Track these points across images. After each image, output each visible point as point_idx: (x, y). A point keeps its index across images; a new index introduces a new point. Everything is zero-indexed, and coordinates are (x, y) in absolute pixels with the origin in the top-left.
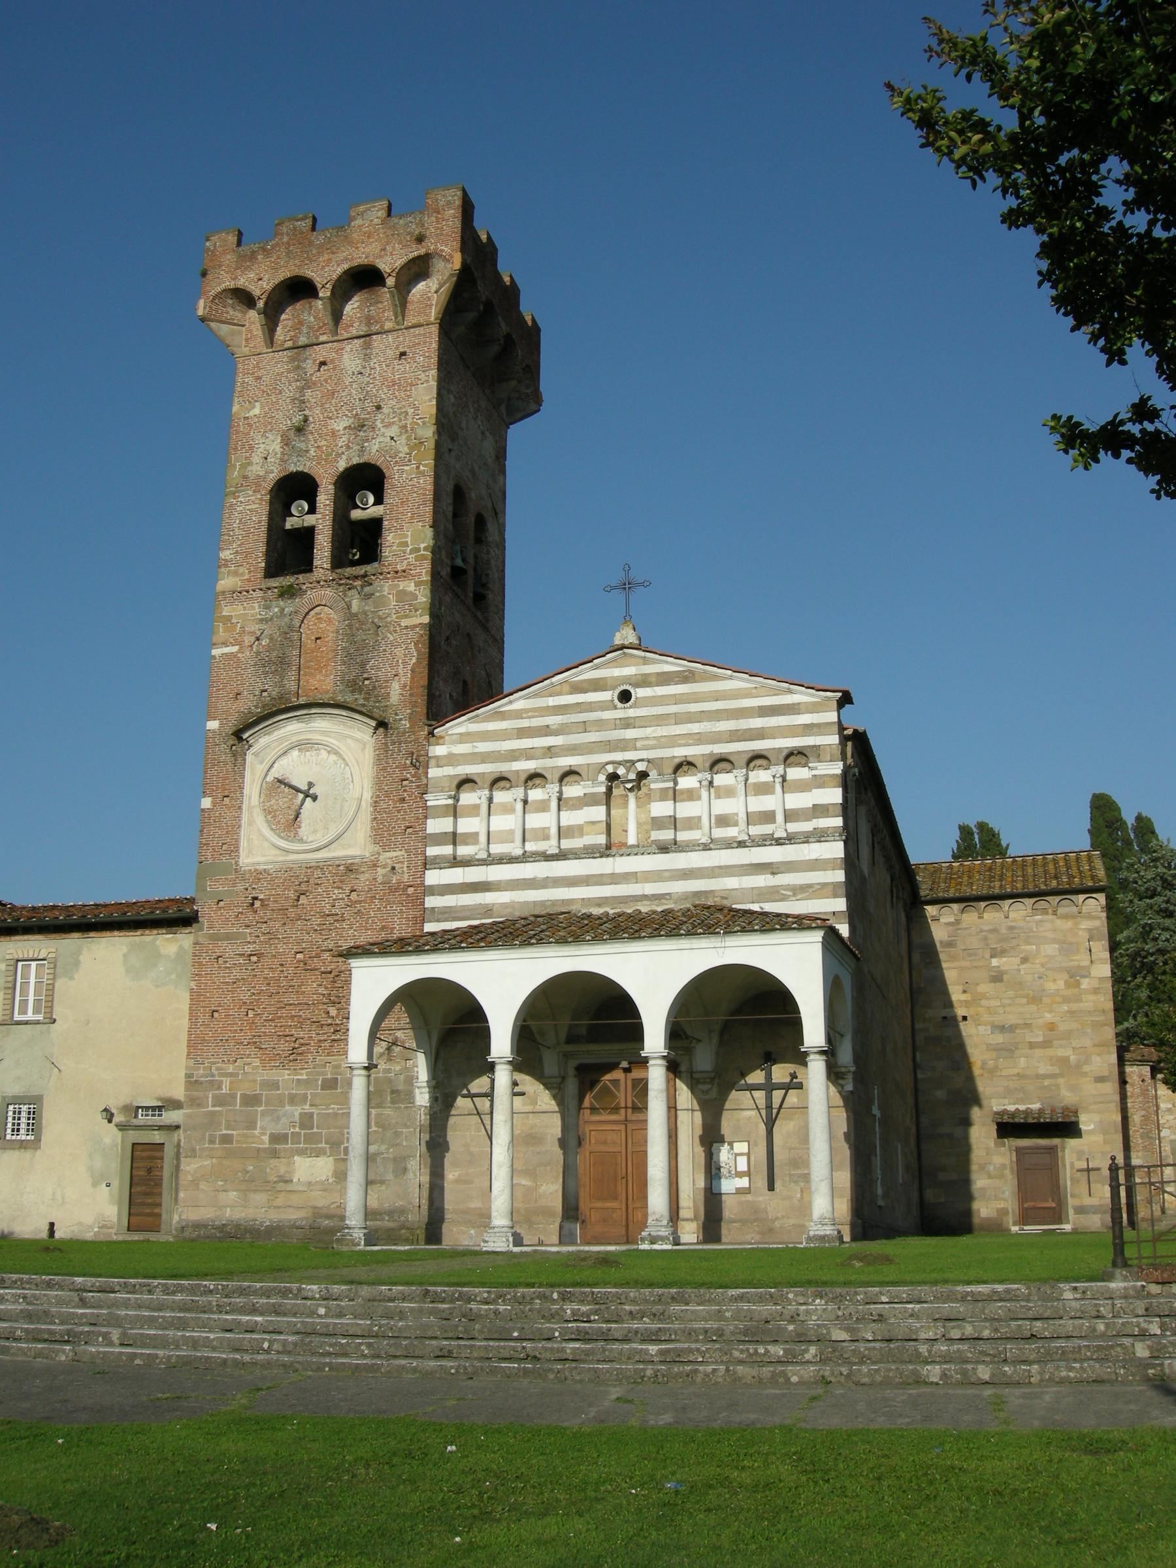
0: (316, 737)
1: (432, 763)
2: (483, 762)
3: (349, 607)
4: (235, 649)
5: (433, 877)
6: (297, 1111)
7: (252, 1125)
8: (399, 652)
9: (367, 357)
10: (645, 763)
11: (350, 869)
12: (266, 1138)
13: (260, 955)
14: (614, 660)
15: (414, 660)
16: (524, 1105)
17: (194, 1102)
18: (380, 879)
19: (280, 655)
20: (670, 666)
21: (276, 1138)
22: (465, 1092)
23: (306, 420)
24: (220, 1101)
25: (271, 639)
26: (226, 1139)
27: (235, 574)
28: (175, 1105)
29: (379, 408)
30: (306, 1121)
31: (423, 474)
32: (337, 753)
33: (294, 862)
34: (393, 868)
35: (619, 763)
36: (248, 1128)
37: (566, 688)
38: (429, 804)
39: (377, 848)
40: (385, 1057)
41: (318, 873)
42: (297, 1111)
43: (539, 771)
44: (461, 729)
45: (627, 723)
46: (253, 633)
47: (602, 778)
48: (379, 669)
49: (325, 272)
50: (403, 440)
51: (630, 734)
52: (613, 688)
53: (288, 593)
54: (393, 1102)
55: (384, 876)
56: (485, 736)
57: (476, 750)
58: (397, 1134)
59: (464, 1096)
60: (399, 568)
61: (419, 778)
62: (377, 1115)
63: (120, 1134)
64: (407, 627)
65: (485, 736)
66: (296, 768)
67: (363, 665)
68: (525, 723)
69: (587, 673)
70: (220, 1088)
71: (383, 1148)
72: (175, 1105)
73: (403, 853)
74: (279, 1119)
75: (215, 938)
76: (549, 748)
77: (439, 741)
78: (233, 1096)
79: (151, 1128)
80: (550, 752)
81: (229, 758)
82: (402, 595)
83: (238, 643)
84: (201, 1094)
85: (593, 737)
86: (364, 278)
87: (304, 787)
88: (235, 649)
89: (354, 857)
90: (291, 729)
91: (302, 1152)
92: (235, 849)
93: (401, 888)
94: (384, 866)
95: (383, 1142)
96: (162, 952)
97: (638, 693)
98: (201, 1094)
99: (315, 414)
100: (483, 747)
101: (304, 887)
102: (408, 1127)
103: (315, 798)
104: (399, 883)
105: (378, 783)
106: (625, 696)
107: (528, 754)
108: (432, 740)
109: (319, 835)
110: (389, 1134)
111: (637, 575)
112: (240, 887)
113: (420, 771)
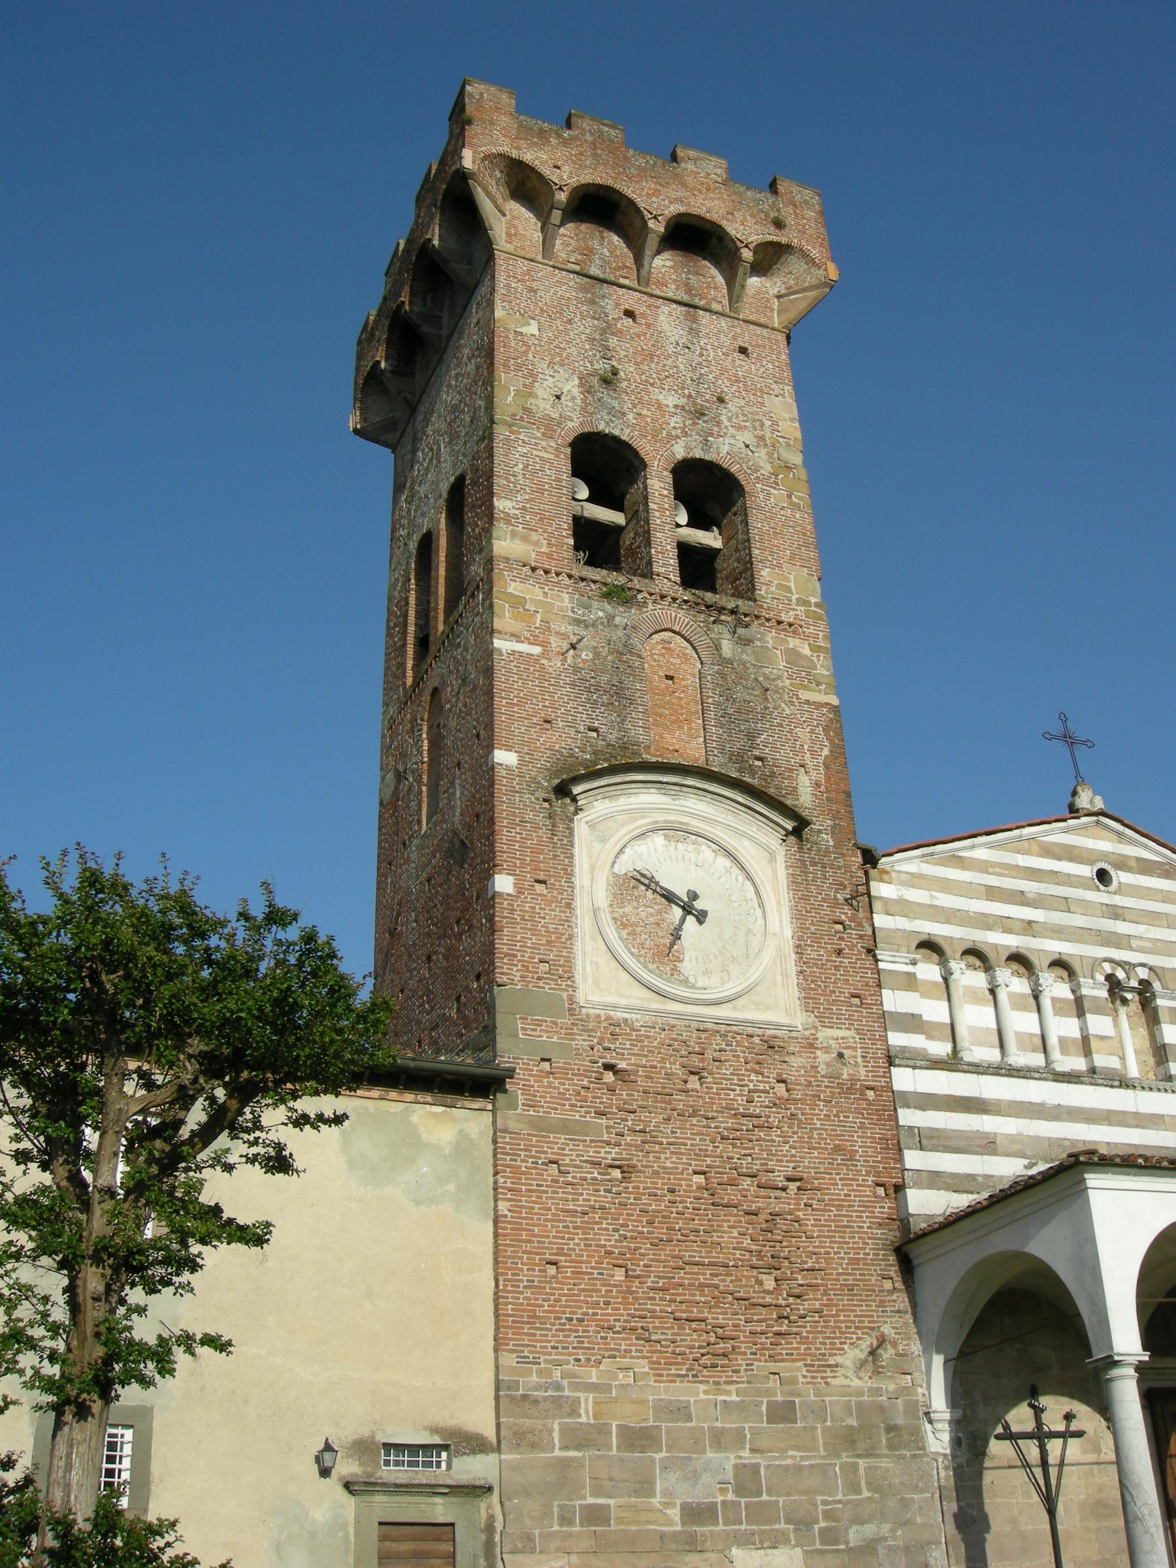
0: (695, 824)
1: (877, 906)
2: (947, 921)
3: (718, 647)
4: (536, 650)
5: (904, 1079)
6: (728, 1461)
7: (645, 1487)
8: (803, 734)
9: (694, 332)
10: (1147, 970)
11: (770, 1046)
12: (675, 1513)
13: (627, 1170)
14: (1085, 827)
15: (826, 752)
16: (1084, 1452)
17: (526, 1440)
18: (823, 1069)
19: (613, 684)
20: (1149, 852)
21: (696, 1513)
22: (999, 1430)
23: (615, 373)
24: (577, 1438)
25: (597, 655)
26: (596, 1515)
27: (525, 539)
28: (476, 1444)
29: (721, 400)
30: (746, 1480)
31: (797, 507)
32: (729, 854)
33: (679, 1016)
34: (841, 1055)
35: (1119, 964)
36: (637, 1493)
37: (1035, 848)
38: (881, 965)
39: (812, 1019)
40: (870, 1367)
41: (717, 1042)
42: (728, 1461)
43: (1022, 951)
44: (912, 867)
45: (1115, 913)
46: (564, 636)
47: (1100, 978)
48: (775, 749)
49: (659, 202)
50: (762, 453)
51: (1122, 927)
52: (1091, 863)
53: (618, 596)
54: (892, 1447)
55: (828, 1065)
56: (945, 886)
57: (936, 903)
58: (905, 1503)
59: (998, 1437)
60: (784, 617)
61: (860, 924)
62: (868, 1469)
63: (349, 1503)
64: (808, 702)
65: (945, 886)
66: (676, 867)
67: (751, 736)
68: (994, 881)
69: (1055, 834)
70: (574, 1412)
71: (886, 1528)
72: (476, 1444)
73: (852, 1033)
74: (696, 1475)
75: (541, 1127)
76: (1030, 922)
77: (884, 876)
78: (602, 1430)
79: (432, 1490)
80: (1029, 927)
81: (540, 819)
82: (793, 656)
83: (544, 644)
84: (538, 1424)
85: (1078, 920)
86: (694, 237)
87: (681, 892)
88: (536, 650)
89: (778, 1026)
90: (645, 801)
91: (744, 1541)
92: (565, 973)
93: (851, 1088)
94: (827, 1050)
95: (883, 1518)
96: (425, 1137)
97: (1120, 877)
98: (538, 1424)
99: (628, 371)
100: (945, 900)
101: (695, 1061)
102: (922, 1491)
103: (701, 917)
104: (853, 1080)
105: (800, 917)
106: (1103, 876)
107: (1005, 925)
108: (872, 872)
109: (715, 980)
110: (892, 1503)
111: (1078, 729)
112: (581, 1041)
113: (861, 914)
